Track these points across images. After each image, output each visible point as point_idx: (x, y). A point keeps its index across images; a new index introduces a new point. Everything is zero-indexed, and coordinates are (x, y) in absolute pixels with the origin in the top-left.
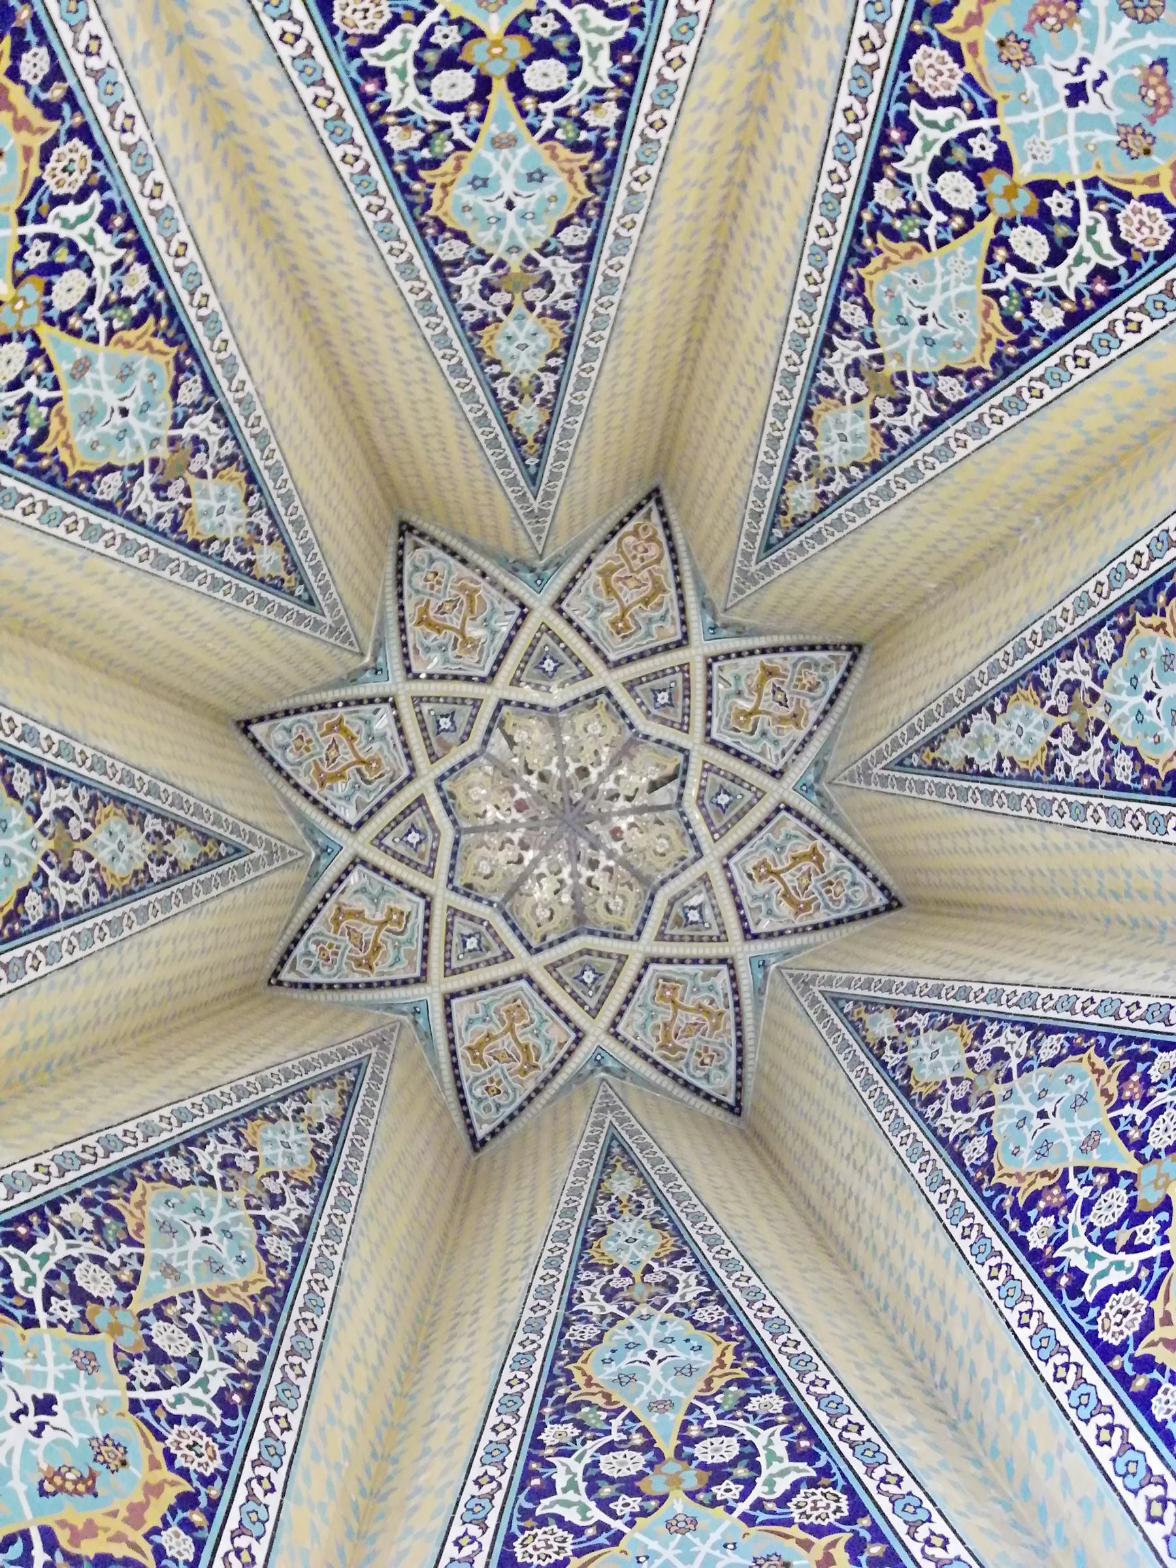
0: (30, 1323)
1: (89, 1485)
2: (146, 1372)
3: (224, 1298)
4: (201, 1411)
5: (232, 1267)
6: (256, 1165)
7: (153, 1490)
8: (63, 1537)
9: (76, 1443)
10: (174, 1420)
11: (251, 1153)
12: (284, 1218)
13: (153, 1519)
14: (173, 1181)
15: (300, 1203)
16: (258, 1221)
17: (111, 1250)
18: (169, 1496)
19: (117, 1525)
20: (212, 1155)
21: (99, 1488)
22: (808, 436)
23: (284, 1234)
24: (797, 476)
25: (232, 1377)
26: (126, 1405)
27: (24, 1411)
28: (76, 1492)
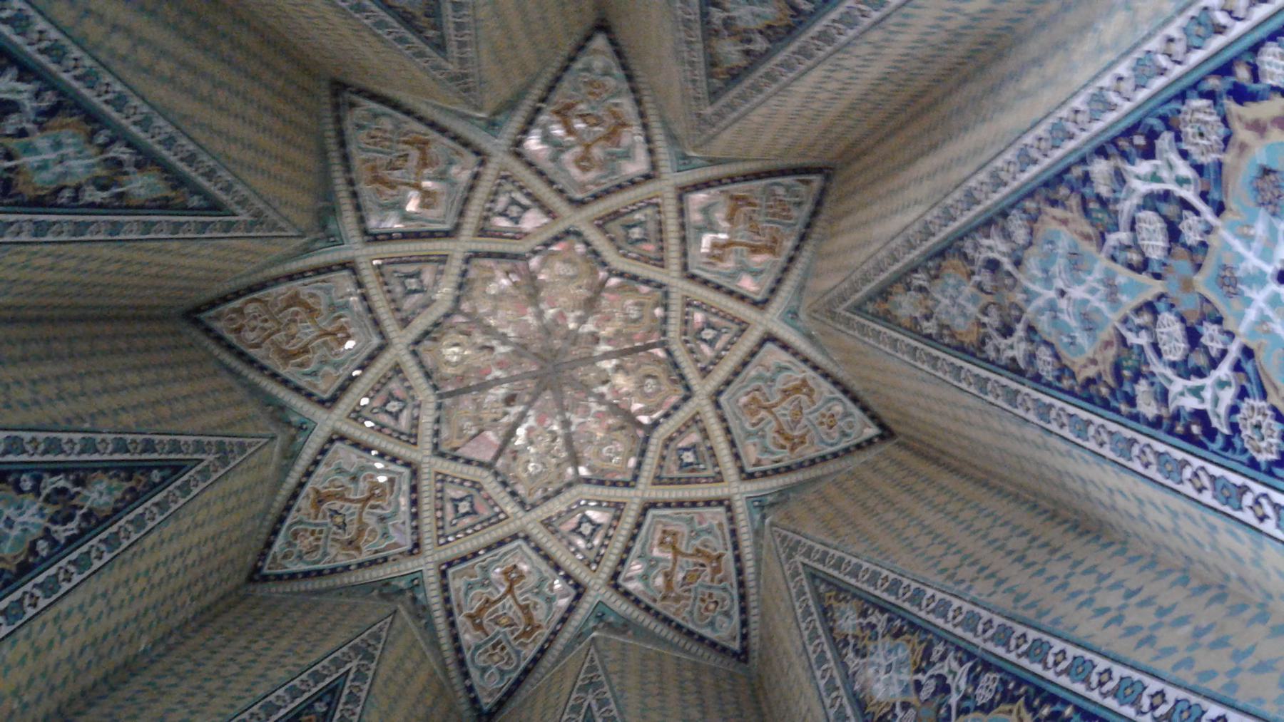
0: (1248, 353)
3: (1088, 229)
5: (1063, 245)
6: (986, 307)
7: (1258, 127)
11: (985, 320)
12: (995, 247)
14: (1056, 356)
16: (1018, 263)
17: (1141, 348)
18: (1251, 111)
22: (43, 547)
23: (1007, 236)
24: (86, 517)
26: (1227, 215)
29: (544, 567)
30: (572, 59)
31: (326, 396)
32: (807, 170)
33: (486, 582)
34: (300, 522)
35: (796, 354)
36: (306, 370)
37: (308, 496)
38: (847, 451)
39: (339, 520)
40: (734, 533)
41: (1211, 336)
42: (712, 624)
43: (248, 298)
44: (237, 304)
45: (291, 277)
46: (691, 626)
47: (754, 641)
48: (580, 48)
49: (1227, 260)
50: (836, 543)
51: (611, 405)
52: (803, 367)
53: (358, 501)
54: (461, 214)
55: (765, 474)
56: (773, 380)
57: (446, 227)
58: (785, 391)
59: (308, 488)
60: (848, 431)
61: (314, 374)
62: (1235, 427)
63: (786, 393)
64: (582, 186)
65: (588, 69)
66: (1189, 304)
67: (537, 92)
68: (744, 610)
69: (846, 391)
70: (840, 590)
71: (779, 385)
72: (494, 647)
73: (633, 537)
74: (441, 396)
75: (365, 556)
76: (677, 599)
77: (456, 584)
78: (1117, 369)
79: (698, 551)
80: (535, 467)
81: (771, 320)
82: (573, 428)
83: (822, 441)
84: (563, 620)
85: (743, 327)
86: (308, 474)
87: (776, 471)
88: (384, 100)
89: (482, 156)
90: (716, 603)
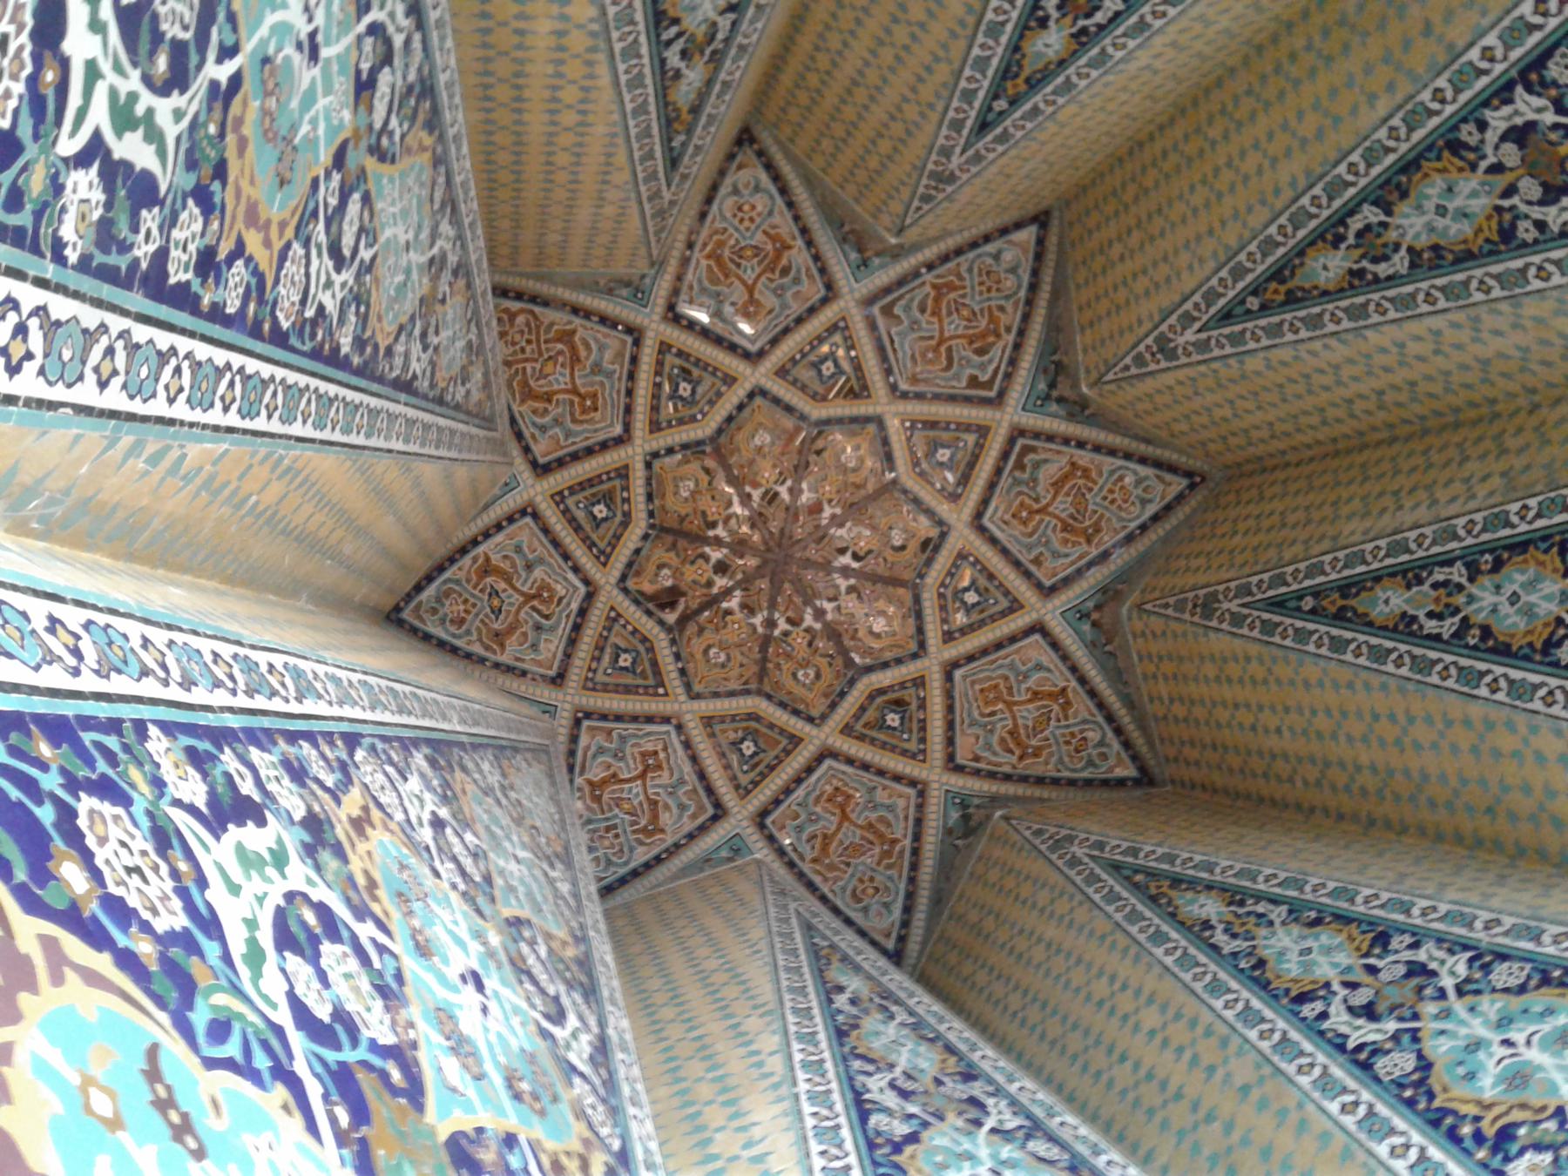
29: (687, 768)
30: (987, 239)
31: (542, 461)
32: (1172, 469)
33: (618, 755)
34: (458, 582)
35: (1065, 657)
36: (539, 420)
37: (475, 560)
38: (1089, 783)
39: (496, 602)
40: (919, 822)
42: (865, 910)
43: (530, 306)
44: (515, 306)
45: (575, 310)
46: (839, 903)
47: (913, 947)
48: (1004, 231)
51: (826, 625)
52: (1068, 674)
53: (523, 594)
54: (774, 342)
55: (977, 773)
56: (1026, 677)
57: (753, 348)
58: (1036, 693)
59: (481, 549)
61: (543, 429)
63: (1036, 695)
64: (914, 380)
65: (997, 257)
67: (930, 253)
68: (908, 909)
69: (1110, 718)
70: (1176, 882)
71: (1030, 683)
72: (608, 829)
73: (798, 781)
74: (652, 526)
75: (505, 658)
76: (832, 867)
77: (584, 740)
79: (871, 825)
80: (717, 655)
81: (1052, 612)
82: (777, 633)
83: (1061, 761)
84: (691, 837)
85: (1015, 606)
86: (487, 535)
87: (992, 775)
88: (777, 178)
89: (831, 291)
90: (877, 890)
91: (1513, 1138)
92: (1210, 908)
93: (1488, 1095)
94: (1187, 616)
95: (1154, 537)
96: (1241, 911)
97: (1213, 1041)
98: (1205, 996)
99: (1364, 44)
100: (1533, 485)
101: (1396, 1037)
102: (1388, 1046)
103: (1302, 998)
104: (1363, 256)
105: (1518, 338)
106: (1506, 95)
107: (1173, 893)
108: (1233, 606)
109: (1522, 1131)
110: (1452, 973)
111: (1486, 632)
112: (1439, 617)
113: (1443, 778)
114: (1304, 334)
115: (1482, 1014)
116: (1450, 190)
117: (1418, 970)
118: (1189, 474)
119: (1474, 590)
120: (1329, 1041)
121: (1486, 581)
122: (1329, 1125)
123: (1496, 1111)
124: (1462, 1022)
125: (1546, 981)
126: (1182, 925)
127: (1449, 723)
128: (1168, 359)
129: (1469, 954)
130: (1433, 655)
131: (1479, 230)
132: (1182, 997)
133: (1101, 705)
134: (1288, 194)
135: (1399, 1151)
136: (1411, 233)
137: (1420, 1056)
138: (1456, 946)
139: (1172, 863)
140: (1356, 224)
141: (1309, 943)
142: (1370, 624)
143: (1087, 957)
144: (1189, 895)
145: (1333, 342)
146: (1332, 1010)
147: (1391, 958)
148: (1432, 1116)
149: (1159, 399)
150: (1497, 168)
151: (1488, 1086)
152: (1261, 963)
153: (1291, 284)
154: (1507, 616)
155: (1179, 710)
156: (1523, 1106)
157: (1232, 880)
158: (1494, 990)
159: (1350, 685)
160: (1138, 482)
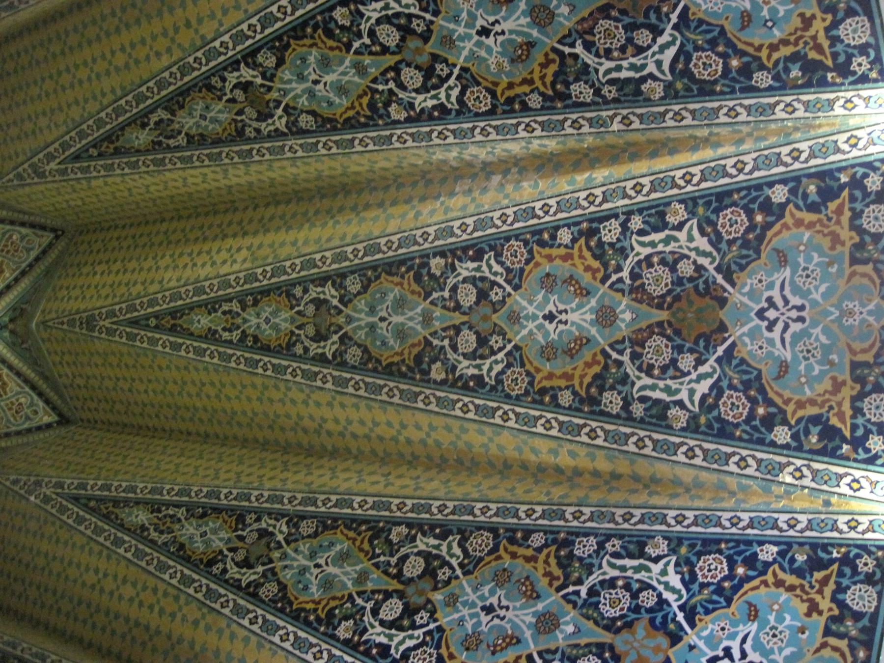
1: (571, 280)
2: (495, 295)
4: (493, 262)
7: (550, 258)
8: (600, 275)
9: (556, 297)
10: (508, 270)
12: (330, 293)
13: (562, 251)
15: (306, 291)
17: (443, 347)
18: (547, 251)
19: (577, 261)
20: (324, 347)
21: (567, 275)
25: (460, 260)
27: (560, 322)
28: (577, 282)
32: (43, 228)
38: (29, 431)
41: (495, 341)
49: (515, 308)
50: (92, 476)
60: (32, 416)
62: (499, 381)
66: (484, 327)
69: (33, 387)
70: (116, 502)
78: (418, 359)
83: (8, 421)
91: (335, 616)
92: (142, 517)
93: (316, 597)
94: (77, 330)
95: (38, 271)
96: (160, 515)
97: (170, 600)
98: (158, 573)
99: (149, 23)
100: (267, 257)
101: (264, 575)
102: (262, 580)
103: (211, 563)
104: (160, 134)
105: (248, 178)
106: (235, 66)
107: (117, 511)
108: (107, 323)
109: (337, 611)
110: (281, 532)
111: (256, 339)
112: (230, 331)
113: (244, 413)
114: (127, 171)
115: (302, 552)
116: (207, 107)
117: (264, 534)
118: (54, 230)
119: (245, 315)
120: (232, 585)
121: (251, 310)
122: (246, 633)
123: (324, 603)
124: (294, 559)
125: (326, 528)
126: (128, 531)
127: (244, 387)
128: (38, 177)
129: (286, 519)
130: (230, 351)
131: (225, 130)
132: (144, 576)
133: (26, 381)
134: (110, 97)
135: (285, 637)
136: (187, 127)
137: (279, 583)
138: (278, 515)
139: (110, 490)
140: (154, 118)
141: (204, 529)
142: (192, 334)
143: (75, 560)
144: (127, 510)
145: (146, 176)
146: (228, 567)
147: (248, 530)
148: (294, 614)
149: (34, 197)
150: (233, 101)
151: (315, 591)
152: (182, 547)
153: (118, 144)
154: (265, 330)
155: (80, 381)
156: (334, 598)
157: (149, 496)
158: (303, 538)
159: (186, 368)
160: (23, 238)
